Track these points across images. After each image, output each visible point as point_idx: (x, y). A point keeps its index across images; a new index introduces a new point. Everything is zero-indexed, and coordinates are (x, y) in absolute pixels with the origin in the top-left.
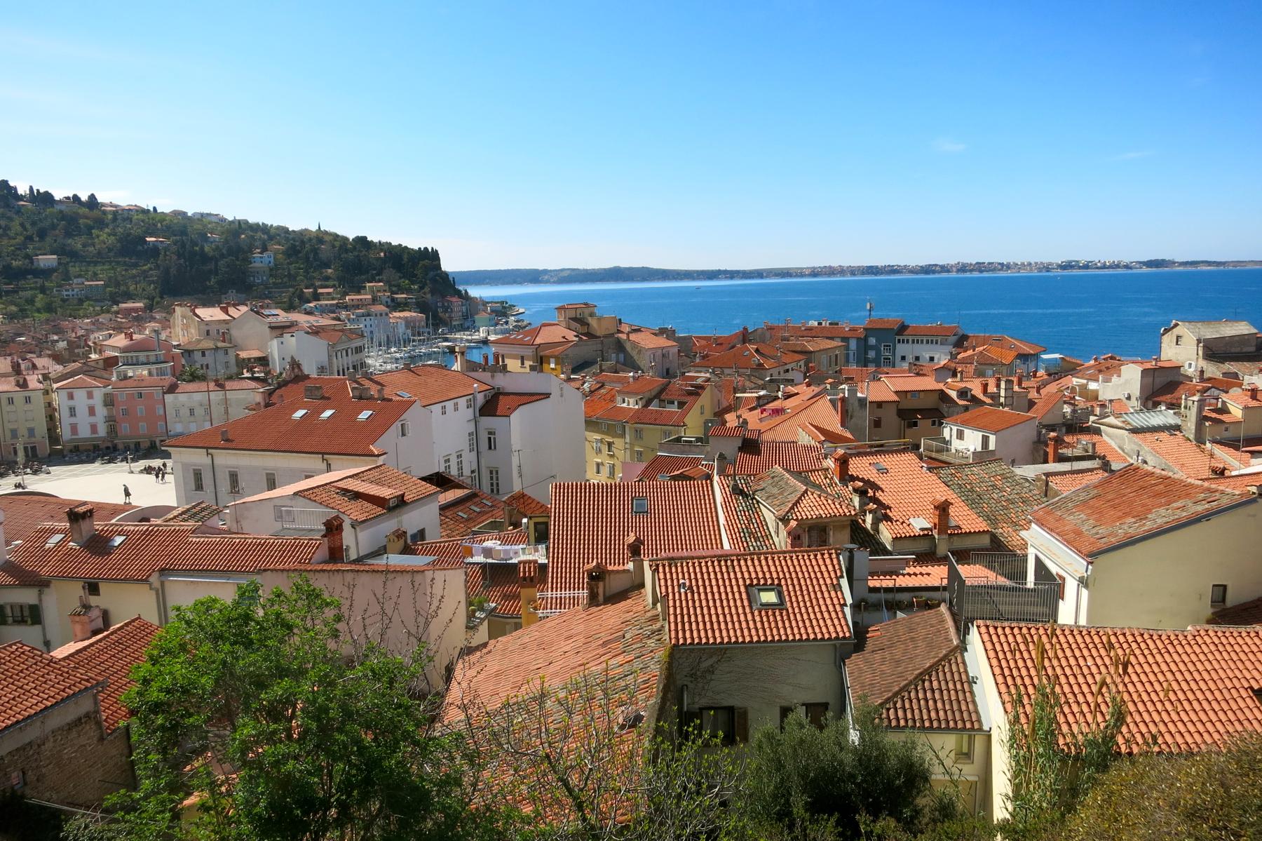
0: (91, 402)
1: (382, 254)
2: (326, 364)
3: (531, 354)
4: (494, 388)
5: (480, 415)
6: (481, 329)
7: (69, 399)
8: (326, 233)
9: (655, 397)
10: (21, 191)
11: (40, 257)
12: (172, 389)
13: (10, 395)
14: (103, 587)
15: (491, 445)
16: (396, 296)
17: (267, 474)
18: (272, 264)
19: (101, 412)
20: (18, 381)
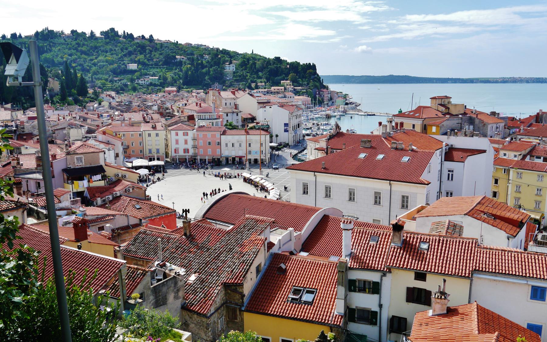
0: (186, 137)
1: (288, 66)
3: (420, 123)
4: (448, 145)
5: (445, 160)
8: (256, 55)
9: (528, 154)
10: (120, 33)
11: (130, 65)
12: (224, 133)
13: (149, 132)
14: (429, 277)
15: (450, 177)
16: (296, 88)
17: (349, 189)
18: (234, 70)
19: (190, 143)
20: (153, 125)
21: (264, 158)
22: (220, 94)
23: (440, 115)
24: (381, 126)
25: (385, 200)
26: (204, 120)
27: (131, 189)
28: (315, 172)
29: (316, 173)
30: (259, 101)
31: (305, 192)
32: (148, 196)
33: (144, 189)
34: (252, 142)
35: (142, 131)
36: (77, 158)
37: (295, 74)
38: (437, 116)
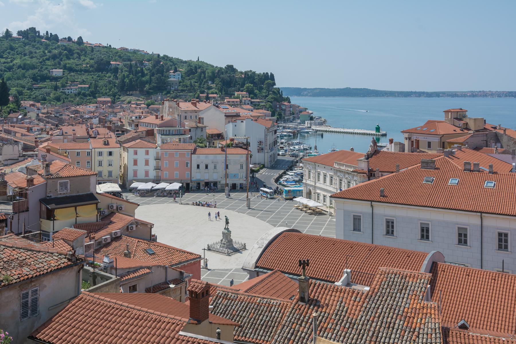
0: (147, 157)
1: (243, 76)
2: (263, 139)
3: (437, 141)
6: (306, 122)
7: (134, 154)
12: (194, 152)
16: (253, 100)
17: (421, 223)
19: (153, 163)
20: (105, 142)
21: (244, 182)
22: (179, 106)
23: (458, 131)
24: (393, 144)
25: (473, 239)
26: (168, 135)
27: (134, 226)
28: (372, 201)
29: (373, 203)
30: (227, 114)
31: (357, 228)
32: (154, 236)
33: (149, 226)
34: (230, 163)
35: (91, 148)
36: (61, 183)
37: (252, 85)
38: (455, 132)
